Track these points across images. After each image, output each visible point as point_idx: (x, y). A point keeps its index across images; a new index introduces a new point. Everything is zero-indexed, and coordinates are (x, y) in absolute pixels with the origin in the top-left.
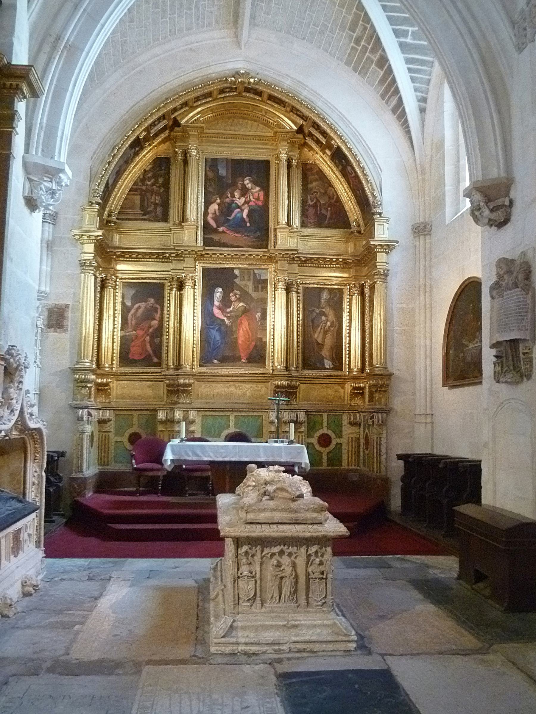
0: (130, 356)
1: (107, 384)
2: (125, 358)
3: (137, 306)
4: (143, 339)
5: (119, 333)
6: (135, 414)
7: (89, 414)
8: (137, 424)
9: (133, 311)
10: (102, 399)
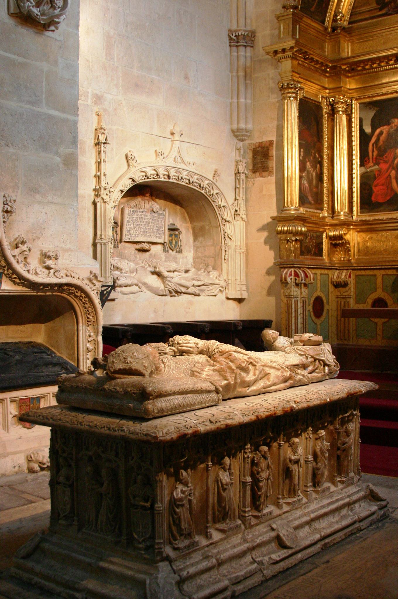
0: (373, 199)
1: (341, 237)
2: (368, 203)
3: (378, 131)
4: (388, 174)
5: (357, 171)
6: (379, 274)
7: (296, 275)
8: (381, 286)
9: (374, 139)
10: (339, 256)
